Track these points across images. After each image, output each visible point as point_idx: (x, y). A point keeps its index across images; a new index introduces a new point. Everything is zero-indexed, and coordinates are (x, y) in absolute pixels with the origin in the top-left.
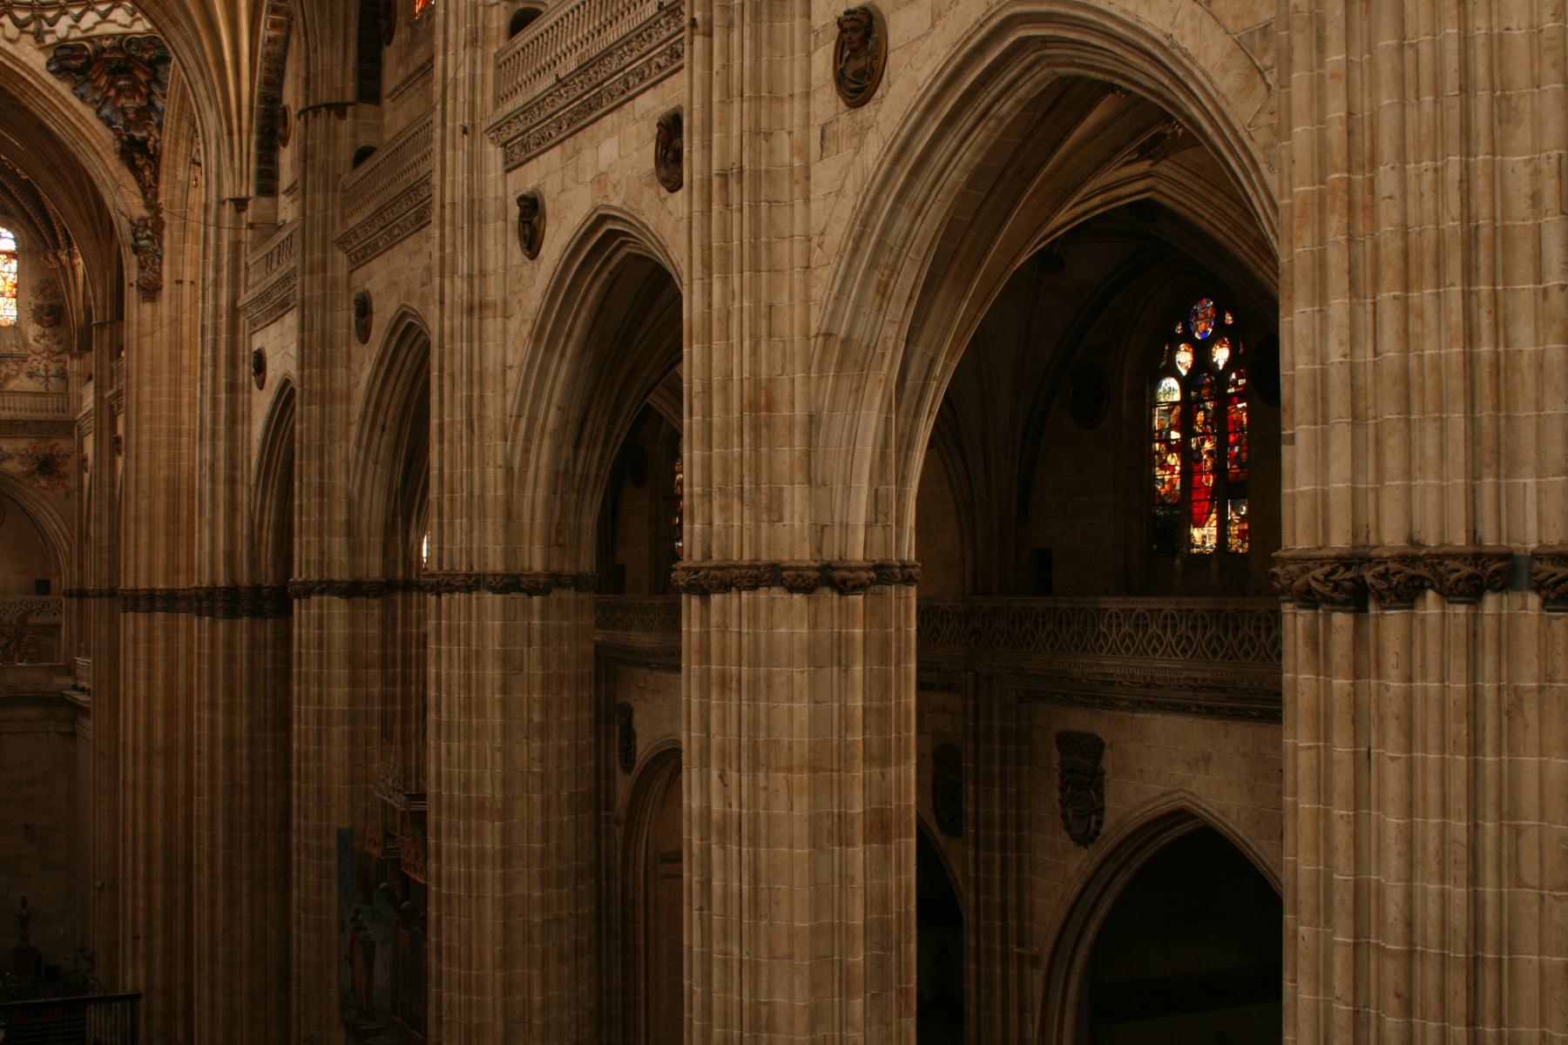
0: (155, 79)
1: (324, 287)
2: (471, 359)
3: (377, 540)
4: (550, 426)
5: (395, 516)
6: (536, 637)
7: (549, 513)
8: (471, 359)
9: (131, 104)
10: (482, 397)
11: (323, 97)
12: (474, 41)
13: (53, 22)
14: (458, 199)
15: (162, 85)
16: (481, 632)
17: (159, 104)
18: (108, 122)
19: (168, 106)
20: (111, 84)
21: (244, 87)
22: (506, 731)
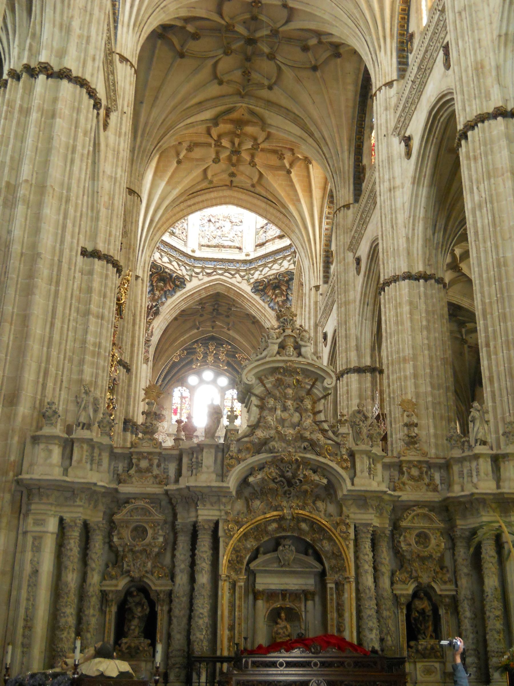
0: (289, 288)
1: (345, 266)
2: (391, 206)
3: (368, 351)
4: (421, 216)
5: (374, 343)
6: (422, 294)
7: (424, 253)
8: (391, 206)
9: (279, 299)
10: (396, 217)
11: (342, 204)
12: (386, 109)
13: (253, 275)
14: (384, 159)
15: (291, 290)
16: (400, 295)
17: (290, 298)
18: (273, 309)
19: (293, 297)
20: (273, 294)
21: (318, 248)
22: (413, 329)
